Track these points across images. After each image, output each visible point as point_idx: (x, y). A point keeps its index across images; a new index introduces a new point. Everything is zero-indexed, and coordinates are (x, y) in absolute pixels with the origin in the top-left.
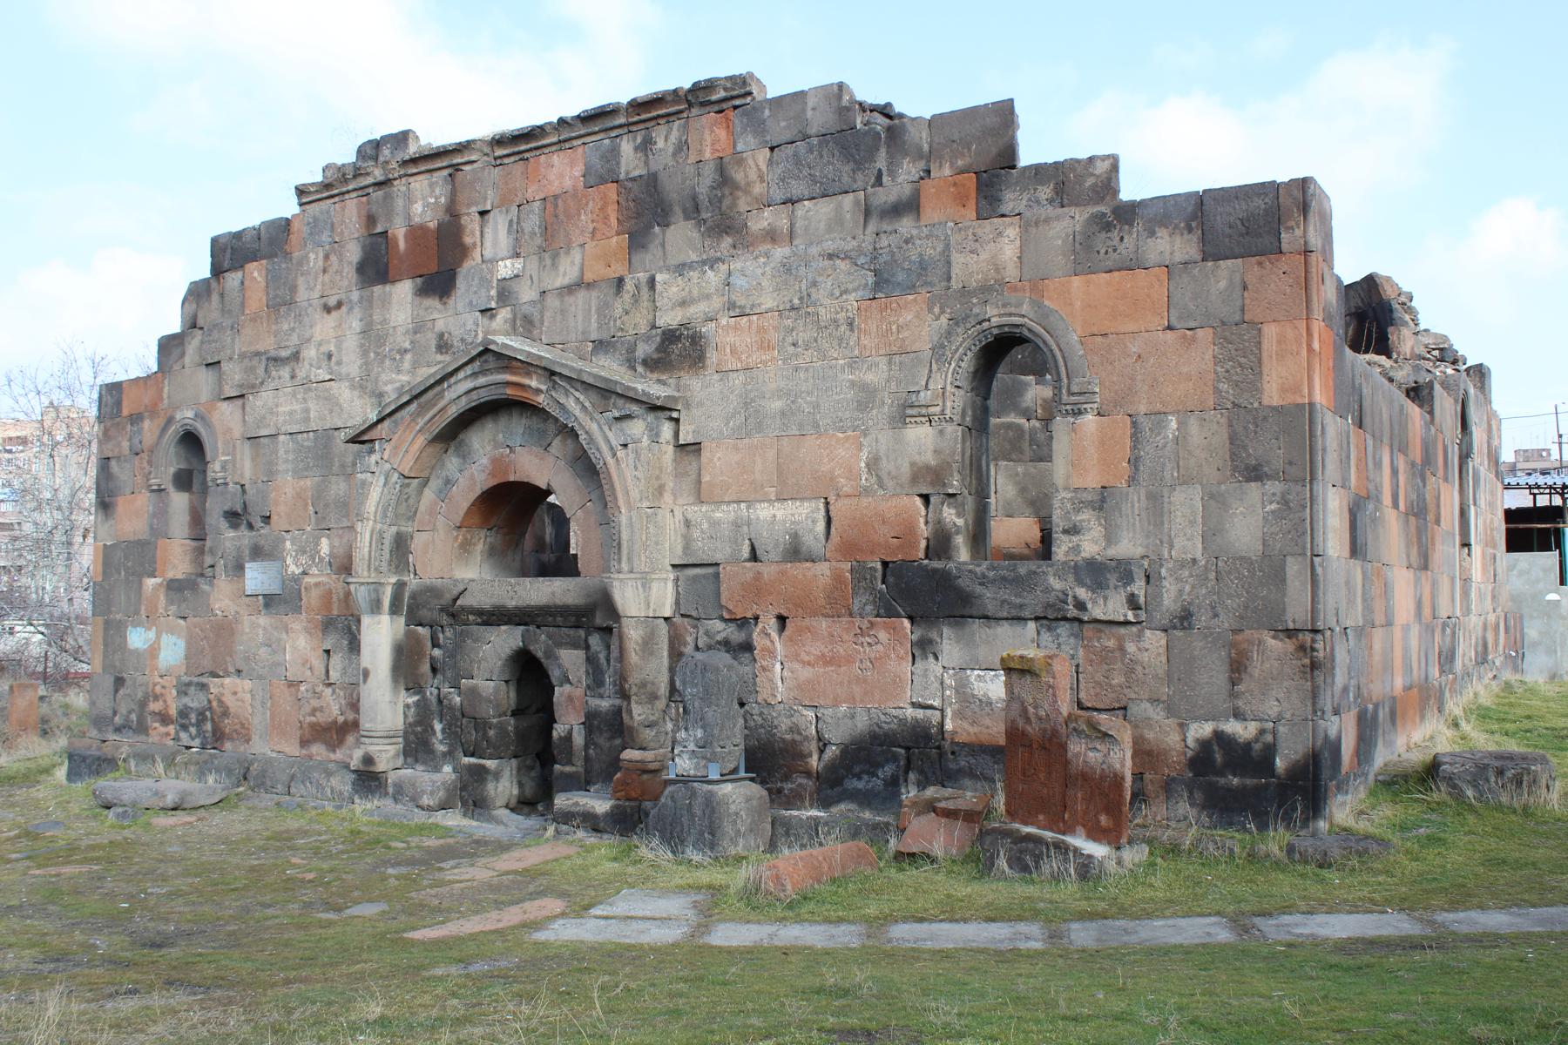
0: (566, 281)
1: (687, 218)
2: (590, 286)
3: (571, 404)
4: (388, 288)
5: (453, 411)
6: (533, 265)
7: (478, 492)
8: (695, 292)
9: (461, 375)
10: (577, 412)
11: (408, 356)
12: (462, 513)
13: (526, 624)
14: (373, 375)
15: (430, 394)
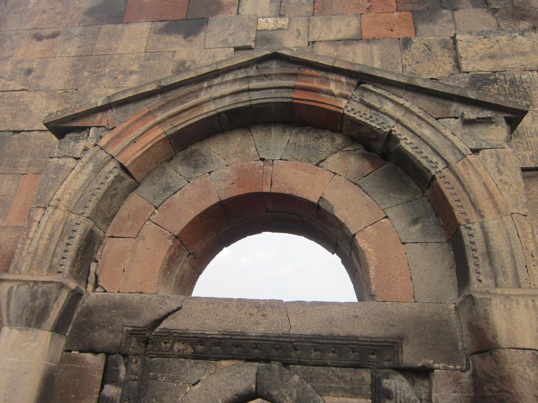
0: (341, 36)
1: (476, 6)
2: (368, 41)
3: (388, 107)
4: (120, 27)
5: (210, 109)
6: (300, 24)
7: (214, 200)
8: (507, 50)
9: (230, 77)
10: (399, 114)
11: (135, 77)
12: (185, 221)
13: (267, 361)
14: (81, 89)
15: (183, 91)
